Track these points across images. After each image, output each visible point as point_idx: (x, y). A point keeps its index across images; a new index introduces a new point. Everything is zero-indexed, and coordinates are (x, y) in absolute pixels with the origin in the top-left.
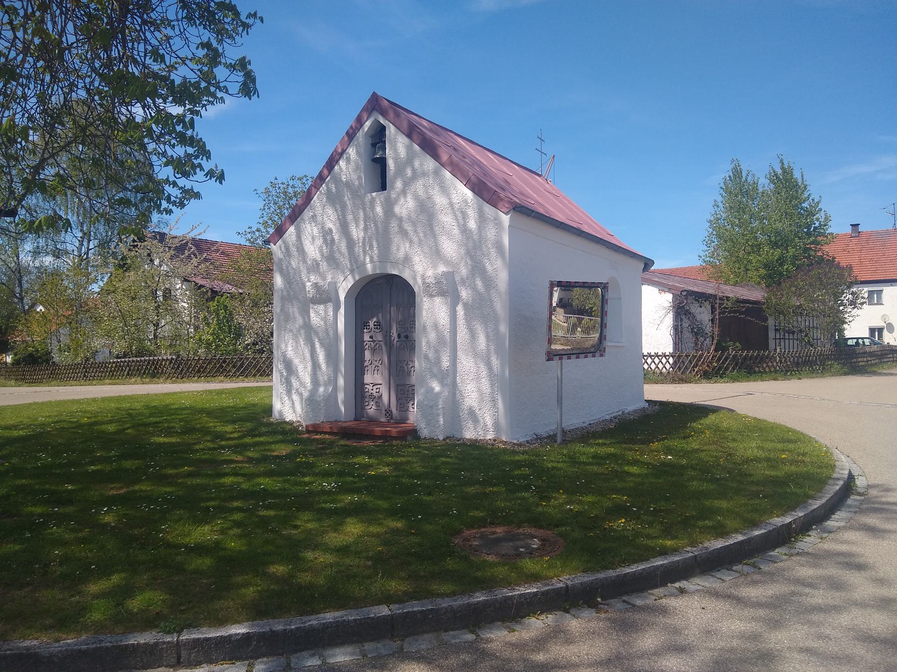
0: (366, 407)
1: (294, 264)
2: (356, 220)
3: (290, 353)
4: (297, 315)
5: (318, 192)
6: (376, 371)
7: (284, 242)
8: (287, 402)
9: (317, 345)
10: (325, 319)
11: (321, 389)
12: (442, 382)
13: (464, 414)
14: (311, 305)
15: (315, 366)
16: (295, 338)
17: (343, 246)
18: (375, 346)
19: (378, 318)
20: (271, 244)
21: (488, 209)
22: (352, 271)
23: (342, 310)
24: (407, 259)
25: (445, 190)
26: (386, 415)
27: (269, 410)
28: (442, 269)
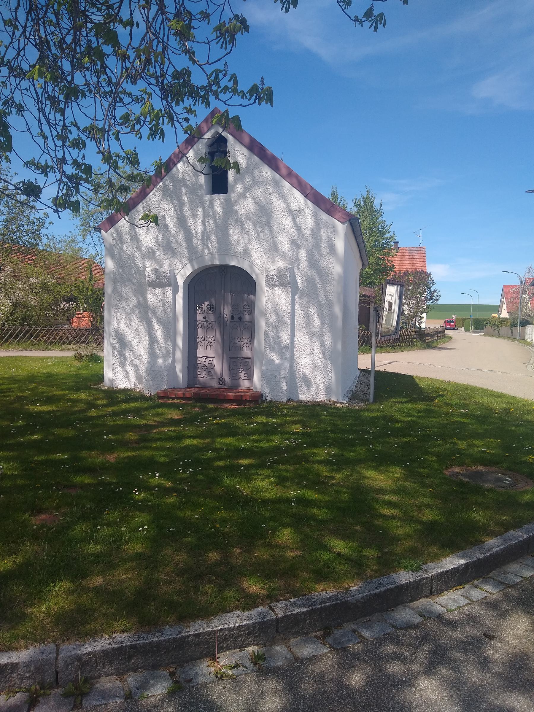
0: (199, 376)
1: (127, 249)
2: (194, 215)
3: (123, 328)
4: (130, 295)
5: (155, 189)
6: (209, 347)
7: (117, 230)
8: (120, 372)
9: (155, 324)
10: (163, 301)
11: (160, 361)
12: (281, 355)
13: (299, 382)
14: (149, 288)
15: (153, 340)
16: (128, 316)
17: (181, 237)
18: (208, 326)
19: (210, 302)
20: (102, 231)
21: (324, 216)
22: (191, 261)
23: (180, 295)
24: (246, 252)
25: (283, 196)
26: (219, 382)
27: (101, 379)
28: (281, 264)
